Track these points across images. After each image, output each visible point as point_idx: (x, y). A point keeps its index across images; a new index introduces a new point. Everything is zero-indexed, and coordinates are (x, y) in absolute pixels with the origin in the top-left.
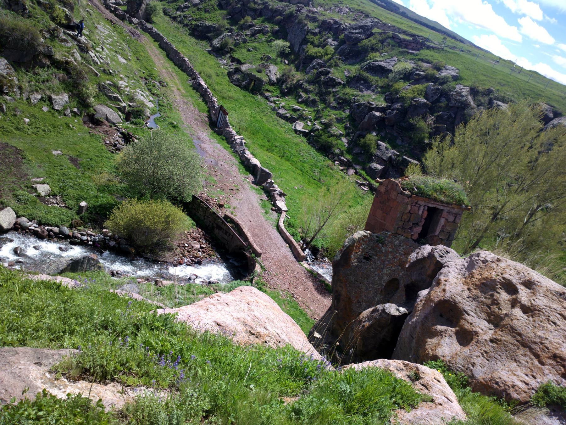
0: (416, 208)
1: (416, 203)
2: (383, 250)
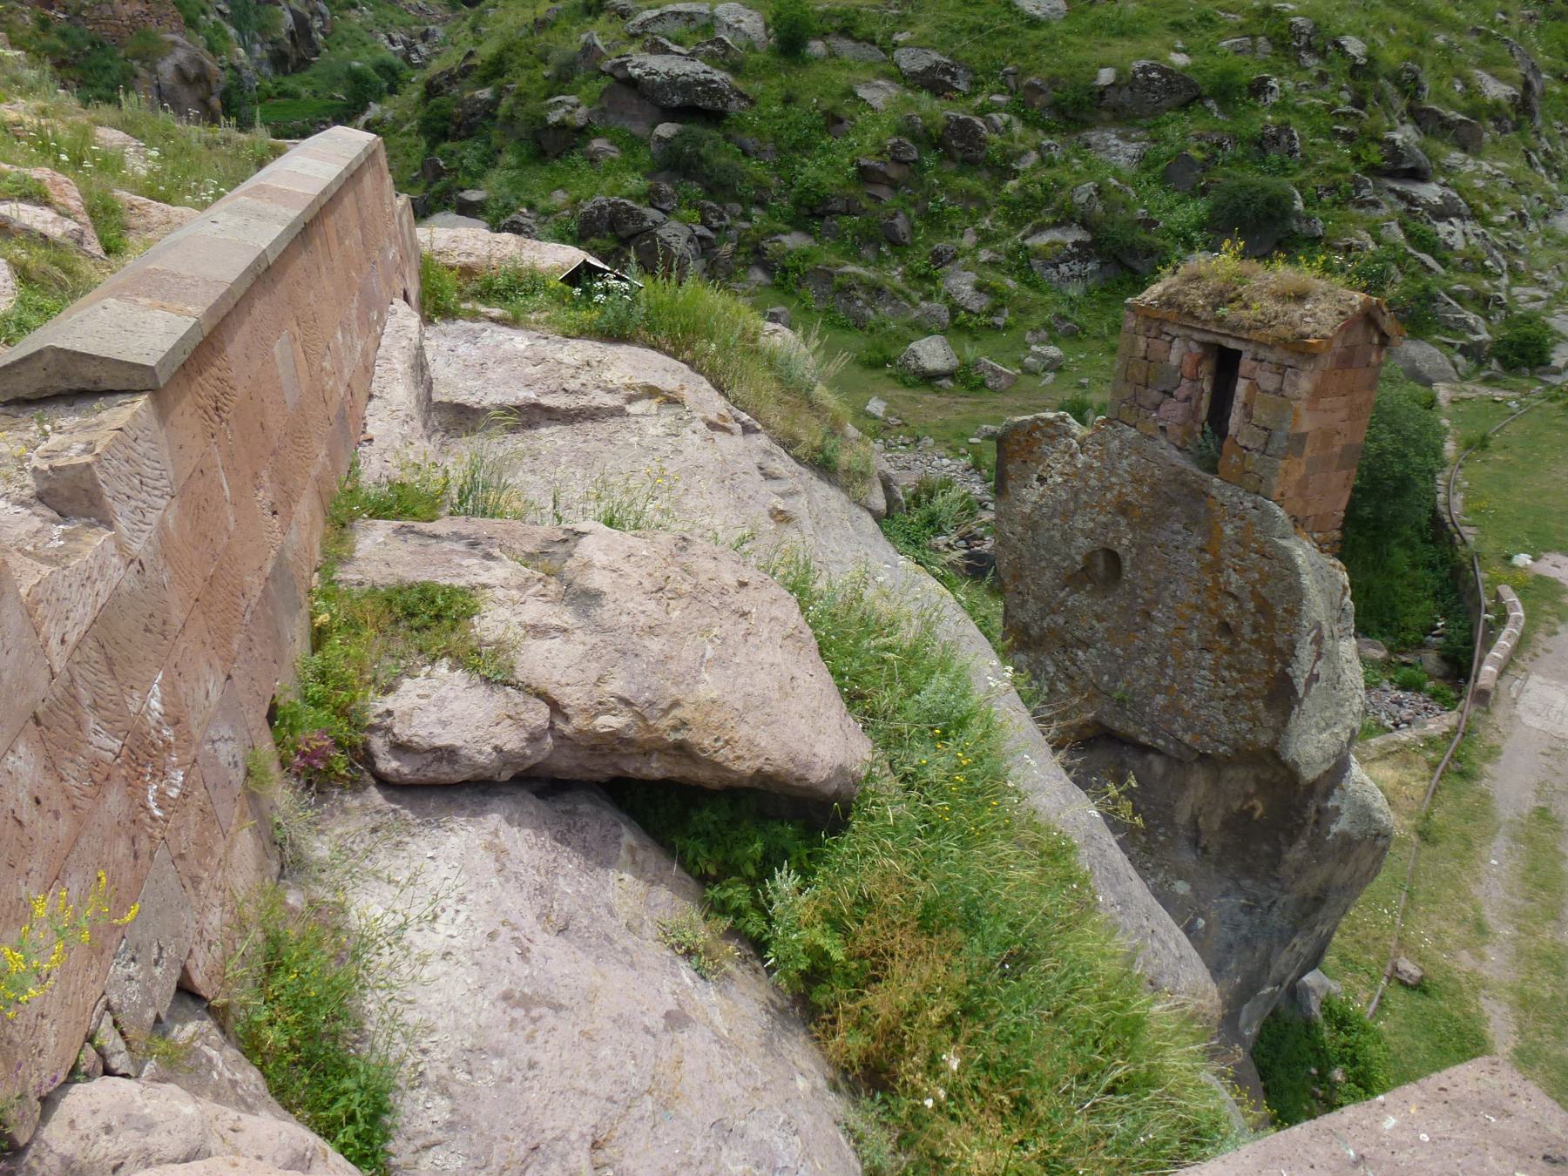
0: (1159, 345)
2: (1081, 458)
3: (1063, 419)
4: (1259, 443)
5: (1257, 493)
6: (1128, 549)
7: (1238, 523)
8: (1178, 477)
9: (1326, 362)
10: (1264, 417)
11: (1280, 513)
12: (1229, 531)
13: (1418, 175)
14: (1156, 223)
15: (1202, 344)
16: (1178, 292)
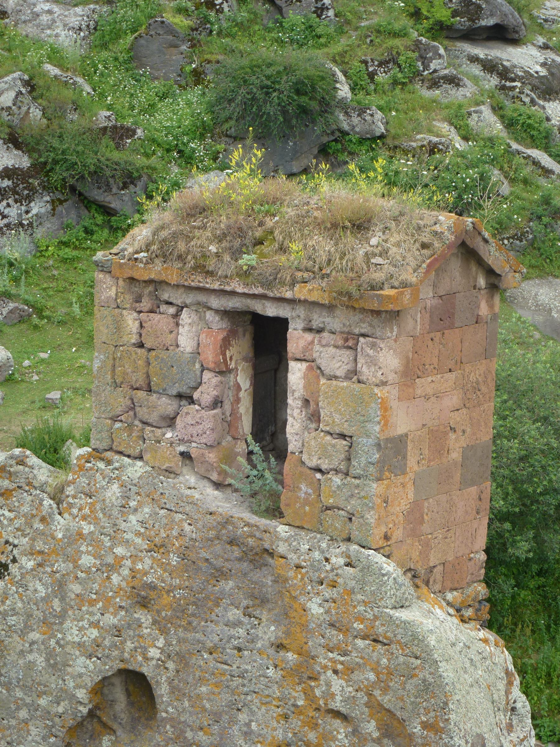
0: (160, 322)
3: (21, 462)
4: (336, 460)
5: (349, 540)
6: (162, 665)
7: (328, 593)
8: (225, 533)
9: (415, 322)
10: (337, 418)
11: (389, 567)
12: (315, 608)
13: (502, 34)
14: (130, 132)
15: (226, 314)
16: (175, 236)
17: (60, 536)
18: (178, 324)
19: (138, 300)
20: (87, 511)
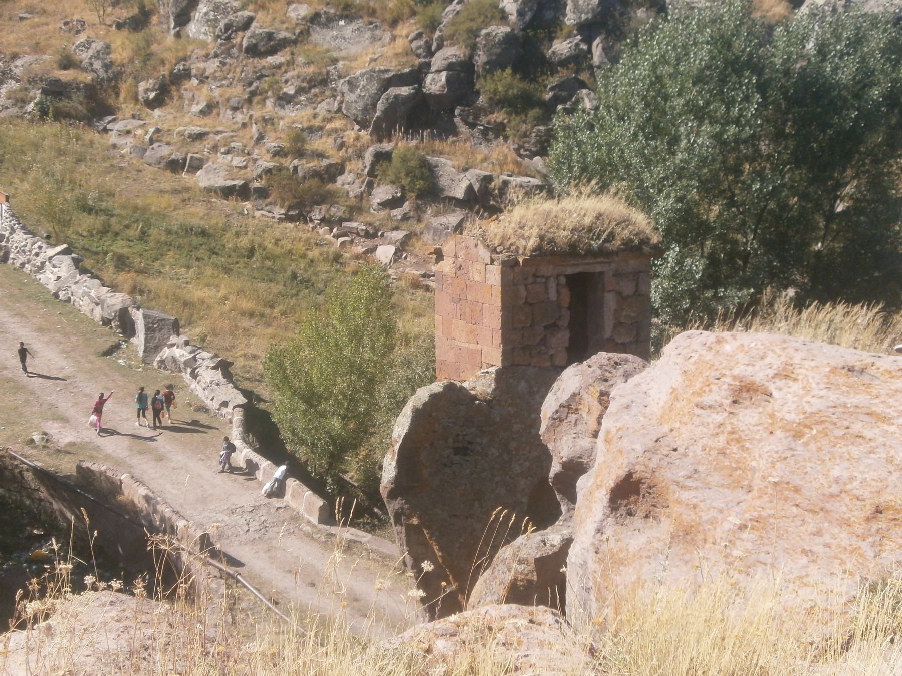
1: (535, 276)
17: (498, 419)
18: (546, 289)
19: (526, 279)
20: (510, 401)
